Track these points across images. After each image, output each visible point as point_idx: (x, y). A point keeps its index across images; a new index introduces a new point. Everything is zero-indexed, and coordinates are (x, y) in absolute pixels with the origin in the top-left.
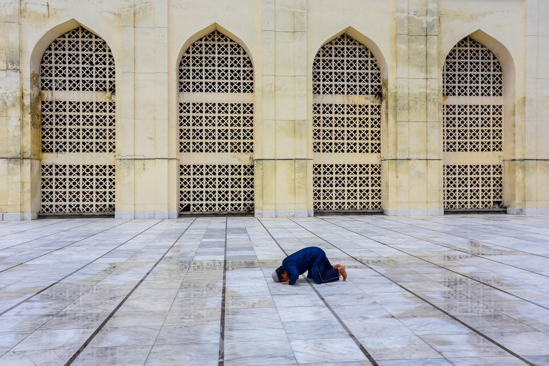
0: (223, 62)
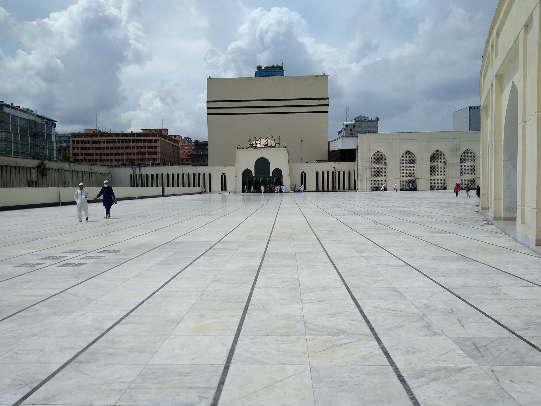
0: (409, 157)
